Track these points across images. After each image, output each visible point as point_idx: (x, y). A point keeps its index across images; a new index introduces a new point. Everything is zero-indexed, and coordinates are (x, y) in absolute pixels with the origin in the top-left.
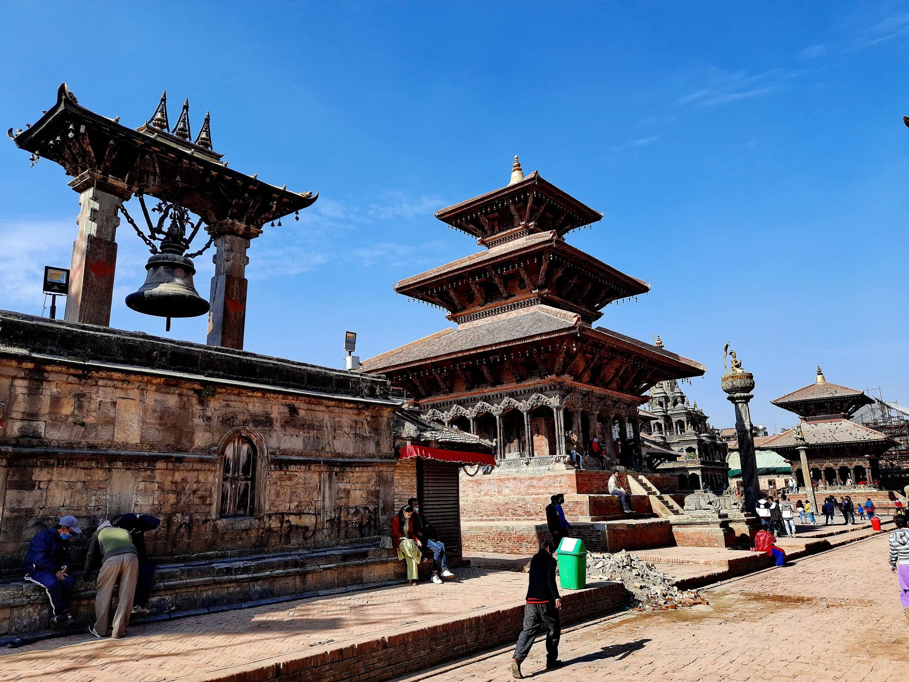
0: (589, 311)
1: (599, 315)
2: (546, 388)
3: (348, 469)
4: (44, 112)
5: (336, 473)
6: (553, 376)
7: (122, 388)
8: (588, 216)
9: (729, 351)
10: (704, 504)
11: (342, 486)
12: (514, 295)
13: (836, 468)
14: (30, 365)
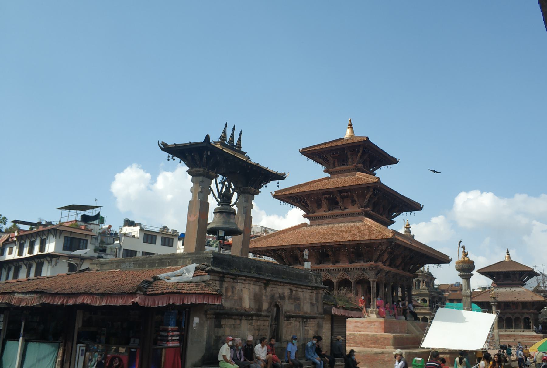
0: (388, 220)
1: (393, 222)
2: (367, 268)
3: (309, 320)
4: (190, 142)
5: (305, 321)
6: (373, 263)
7: (244, 283)
8: (391, 161)
9: (461, 246)
11: (306, 328)
12: (347, 209)
13: (513, 318)
14: (221, 275)
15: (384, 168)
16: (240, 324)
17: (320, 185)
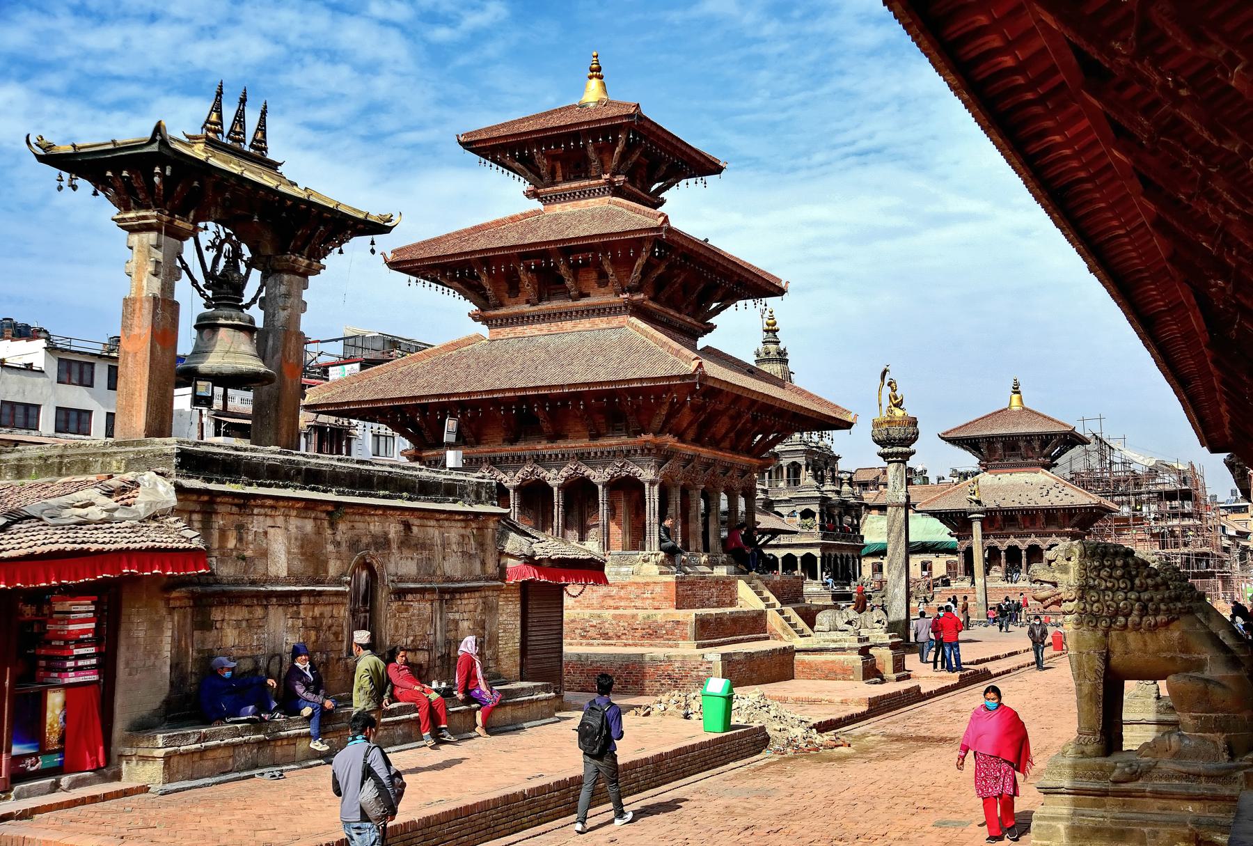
0: (695, 323)
1: (711, 328)
2: (636, 451)
3: (458, 596)
5: (446, 600)
6: (650, 437)
7: (270, 516)
9: (887, 380)
10: (841, 624)
11: (451, 616)
12: (588, 295)
14: (206, 498)
15: (687, 184)
16: (265, 616)
17: (514, 234)
